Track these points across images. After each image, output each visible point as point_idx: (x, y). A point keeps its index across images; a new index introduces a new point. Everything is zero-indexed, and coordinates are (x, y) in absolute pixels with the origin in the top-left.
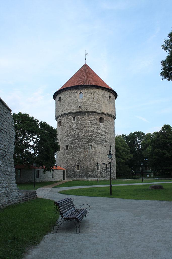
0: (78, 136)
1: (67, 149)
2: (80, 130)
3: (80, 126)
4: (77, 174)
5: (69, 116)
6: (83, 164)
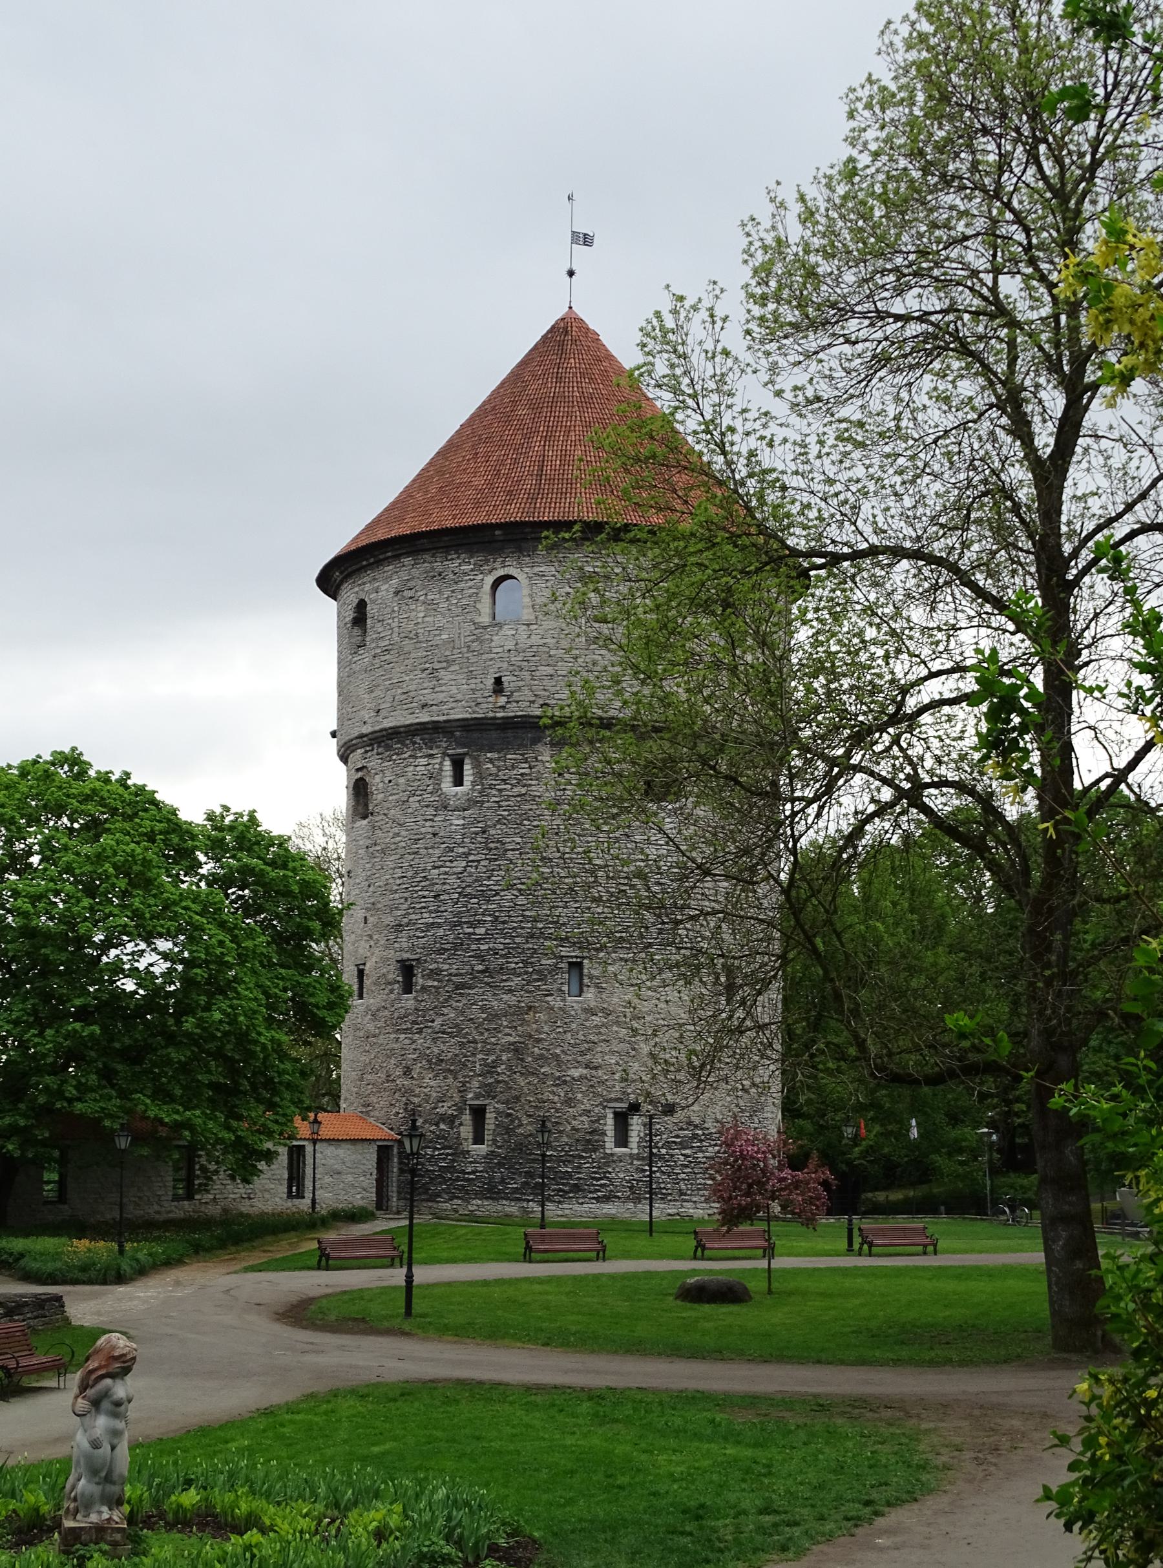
1: (408, 988)
2: (496, 850)
3: (498, 821)
4: (473, 1172)
5: (426, 751)
6: (517, 1099)
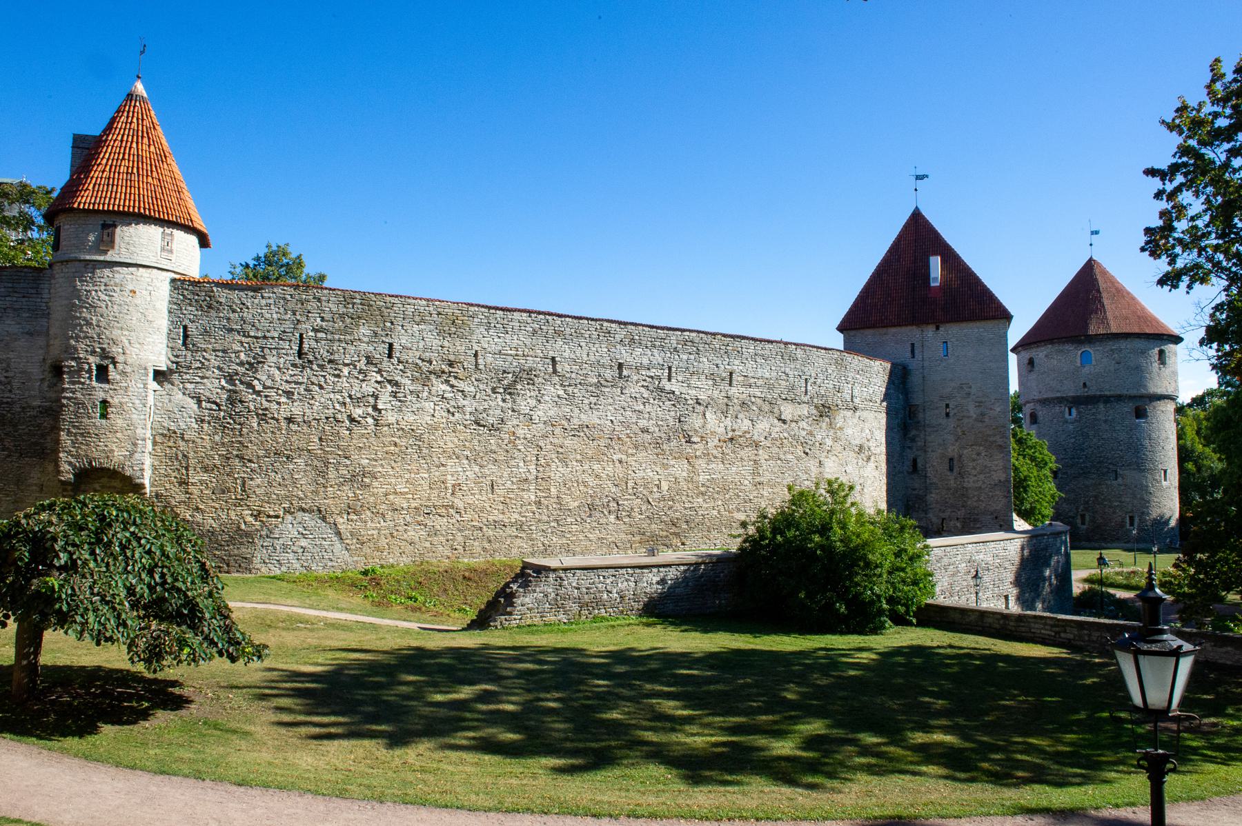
0: (1083, 450)
